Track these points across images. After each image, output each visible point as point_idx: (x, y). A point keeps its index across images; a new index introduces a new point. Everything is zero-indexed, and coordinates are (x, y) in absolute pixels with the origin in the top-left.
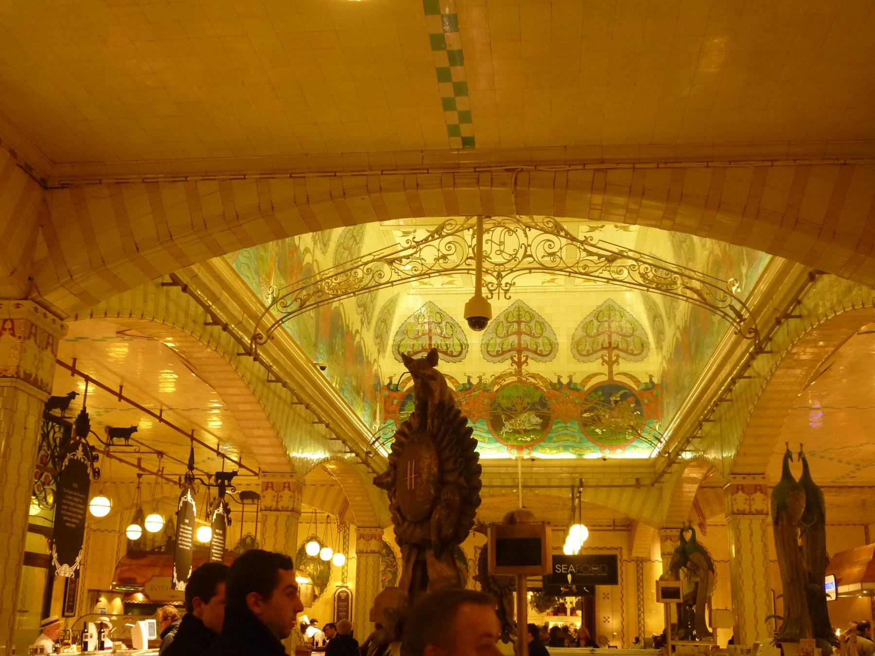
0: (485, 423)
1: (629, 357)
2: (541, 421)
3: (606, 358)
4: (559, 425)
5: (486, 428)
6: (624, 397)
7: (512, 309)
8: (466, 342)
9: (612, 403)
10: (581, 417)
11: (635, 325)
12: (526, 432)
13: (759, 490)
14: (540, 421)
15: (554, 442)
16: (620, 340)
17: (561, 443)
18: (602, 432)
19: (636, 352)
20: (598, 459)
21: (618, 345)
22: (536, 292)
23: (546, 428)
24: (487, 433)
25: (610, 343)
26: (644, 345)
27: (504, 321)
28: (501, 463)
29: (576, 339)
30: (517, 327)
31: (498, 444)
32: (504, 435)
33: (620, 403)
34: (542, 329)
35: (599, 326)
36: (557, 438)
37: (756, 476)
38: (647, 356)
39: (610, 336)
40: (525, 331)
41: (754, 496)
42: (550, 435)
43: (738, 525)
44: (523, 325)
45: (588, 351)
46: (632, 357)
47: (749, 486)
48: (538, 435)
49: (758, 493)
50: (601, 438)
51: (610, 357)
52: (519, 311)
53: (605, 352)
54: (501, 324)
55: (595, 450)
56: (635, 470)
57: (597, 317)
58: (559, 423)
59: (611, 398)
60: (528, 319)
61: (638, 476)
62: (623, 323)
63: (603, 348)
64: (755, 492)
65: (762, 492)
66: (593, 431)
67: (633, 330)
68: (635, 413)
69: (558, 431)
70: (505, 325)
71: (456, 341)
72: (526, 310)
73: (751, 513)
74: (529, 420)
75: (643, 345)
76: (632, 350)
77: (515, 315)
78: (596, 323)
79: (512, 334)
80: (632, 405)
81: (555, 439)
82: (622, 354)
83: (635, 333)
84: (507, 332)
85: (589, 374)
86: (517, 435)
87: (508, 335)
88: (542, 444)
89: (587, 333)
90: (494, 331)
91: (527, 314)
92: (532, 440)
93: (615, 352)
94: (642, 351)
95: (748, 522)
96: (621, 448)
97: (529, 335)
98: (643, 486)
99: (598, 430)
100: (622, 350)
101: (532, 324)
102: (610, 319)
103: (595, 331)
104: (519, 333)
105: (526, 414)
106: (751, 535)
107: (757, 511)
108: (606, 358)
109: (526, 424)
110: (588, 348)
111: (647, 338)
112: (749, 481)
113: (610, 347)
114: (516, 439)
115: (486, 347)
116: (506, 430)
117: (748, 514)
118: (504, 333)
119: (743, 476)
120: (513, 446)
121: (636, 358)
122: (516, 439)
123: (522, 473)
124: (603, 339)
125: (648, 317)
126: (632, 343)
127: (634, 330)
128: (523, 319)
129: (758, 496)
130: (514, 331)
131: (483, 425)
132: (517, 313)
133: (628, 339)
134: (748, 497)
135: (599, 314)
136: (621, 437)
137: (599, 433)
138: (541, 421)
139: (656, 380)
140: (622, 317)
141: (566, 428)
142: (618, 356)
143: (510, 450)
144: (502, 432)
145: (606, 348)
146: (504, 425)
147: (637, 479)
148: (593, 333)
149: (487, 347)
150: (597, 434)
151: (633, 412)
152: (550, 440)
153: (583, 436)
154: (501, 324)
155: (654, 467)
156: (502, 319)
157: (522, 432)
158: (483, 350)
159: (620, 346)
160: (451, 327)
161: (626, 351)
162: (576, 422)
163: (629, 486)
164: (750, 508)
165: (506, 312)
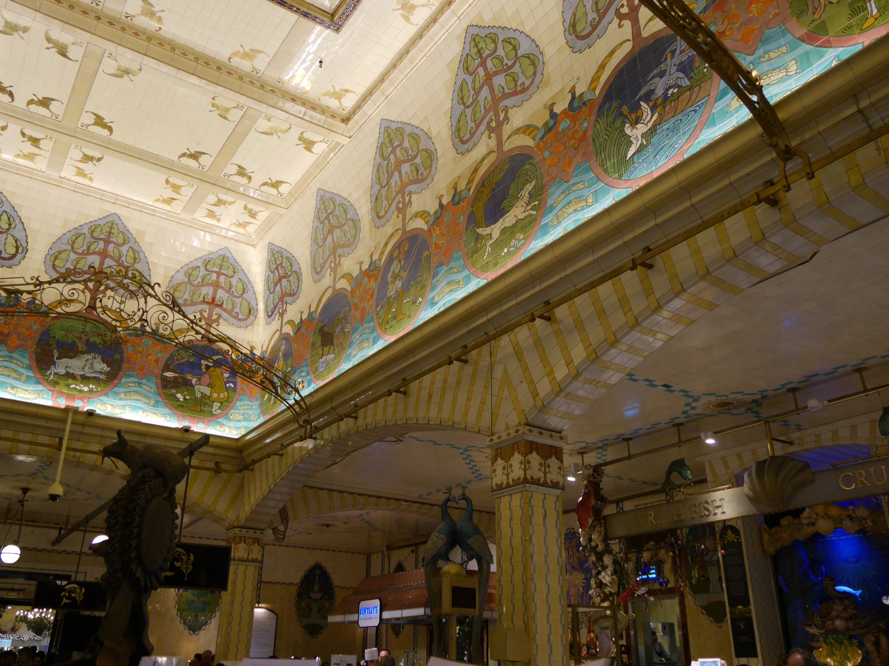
0: (27, 355)
1: (232, 320)
2: (108, 369)
3: (206, 315)
4: (131, 379)
5: (27, 362)
6: (218, 364)
7: (102, 223)
8: (24, 245)
9: (203, 367)
10: (162, 375)
11: (246, 286)
12: (85, 379)
14: (105, 367)
15: (120, 399)
16: (226, 298)
17: (129, 402)
18: (185, 399)
19: (241, 316)
20: (176, 429)
21: (223, 303)
22: (141, 211)
23: (114, 379)
24: (26, 368)
25: (214, 299)
26: (251, 311)
27: (87, 233)
28: (41, 411)
29: (175, 282)
30: (102, 247)
31: (40, 387)
32: (52, 377)
33: (212, 369)
34: (135, 259)
35: (206, 276)
36: (125, 395)
38: (252, 324)
39: (215, 292)
40: (112, 254)
41: (549, 461)
42: (116, 389)
43: (530, 499)
44: (111, 247)
45: (186, 300)
46: (235, 321)
47: (543, 445)
48: (99, 386)
49: (554, 459)
50: (182, 406)
51: (210, 315)
52: (111, 228)
53: (206, 307)
54: (83, 236)
55: (172, 419)
56: (218, 451)
57: (206, 265)
59: (202, 361)
60: (121, 241)
61: (218, 459)
62: (234, 281)
63: (204, 302)
65: (557, 458)
66: (174, 396)
67: (244, 290)
68: (228, 385)
69: (129, 386)
70: (87, 240)
71: (10, 240)
72: (121, 230)
73: (545, 484)
74: (92, 364)
75: (250, 311)
76: (236, 313)
77: (104, 231)
78: (203, 272)
79: (94, 253)
80: (226, 375)
81: (122, 395)
82: (224, 314)
83: (245, 295)
84: (88, 248)
85: (180, 328)
86: (70, 381)
87: (88, 252)
88: (103, 398)
89: (189, 280)
90: (70, 243)
91: (121, 235)
92: (91, 391)
93: (217, 310)
94: (248, 317)
95: (541, 497)
96: (204, 423)
97: (116, 261)
98: (226, 471)
99: (179, 396)
100: (225, 310)
101: (124, 249)
102: (221, 269)
103: (200, 280)
104: (104, 254)
105: (89, 357)
106: (545, 517)
107: (552, 482)
108: (206, 315)
109: (87, 369)
110: (186, 296)
111: (257, 305)
112: (546, 440)
113: (213, 303)
114: (68, 385)
115: (52, 260)
116: (56, 371)
118: (82, 249)
119: (539, 430)
120: (61, 394)
121: (243, 324)
122: (68, 385)
123: (71, 431)
124: (208, 291)
125: (267, 279)
126: (239, 306)
127: (243, 293)
128: (114, 240)
129: (553, 461)
130: (97, 250)
131: (24, 357)
132: (108, 230)
133: (235, 299)
134: (543, 461)
135: (209, 261)
136: (207, 408)
137: (181, 399)
138: (108, 369)
139: (258, 352)
140: (234, 272)
141: (139, 384)
142: (220, 316)
143: (57, 398)
144: (49, 372)
145: (208, 303)
146: (54, 364)
147: (217, 463)
148: (196, 283)
149: (56, 259)
150: (178, 400)
151: (226, 383)
152: (116, 394)
153: (160, 399)
154: (83, 236)
155: (241, 452)
156: (85, 230)
157: (79, 378)
158: (48, 261)
159: (224, 305)
160: (9, 219)
161: (229, 313)
163: (205, 469)
165: (94, 223)
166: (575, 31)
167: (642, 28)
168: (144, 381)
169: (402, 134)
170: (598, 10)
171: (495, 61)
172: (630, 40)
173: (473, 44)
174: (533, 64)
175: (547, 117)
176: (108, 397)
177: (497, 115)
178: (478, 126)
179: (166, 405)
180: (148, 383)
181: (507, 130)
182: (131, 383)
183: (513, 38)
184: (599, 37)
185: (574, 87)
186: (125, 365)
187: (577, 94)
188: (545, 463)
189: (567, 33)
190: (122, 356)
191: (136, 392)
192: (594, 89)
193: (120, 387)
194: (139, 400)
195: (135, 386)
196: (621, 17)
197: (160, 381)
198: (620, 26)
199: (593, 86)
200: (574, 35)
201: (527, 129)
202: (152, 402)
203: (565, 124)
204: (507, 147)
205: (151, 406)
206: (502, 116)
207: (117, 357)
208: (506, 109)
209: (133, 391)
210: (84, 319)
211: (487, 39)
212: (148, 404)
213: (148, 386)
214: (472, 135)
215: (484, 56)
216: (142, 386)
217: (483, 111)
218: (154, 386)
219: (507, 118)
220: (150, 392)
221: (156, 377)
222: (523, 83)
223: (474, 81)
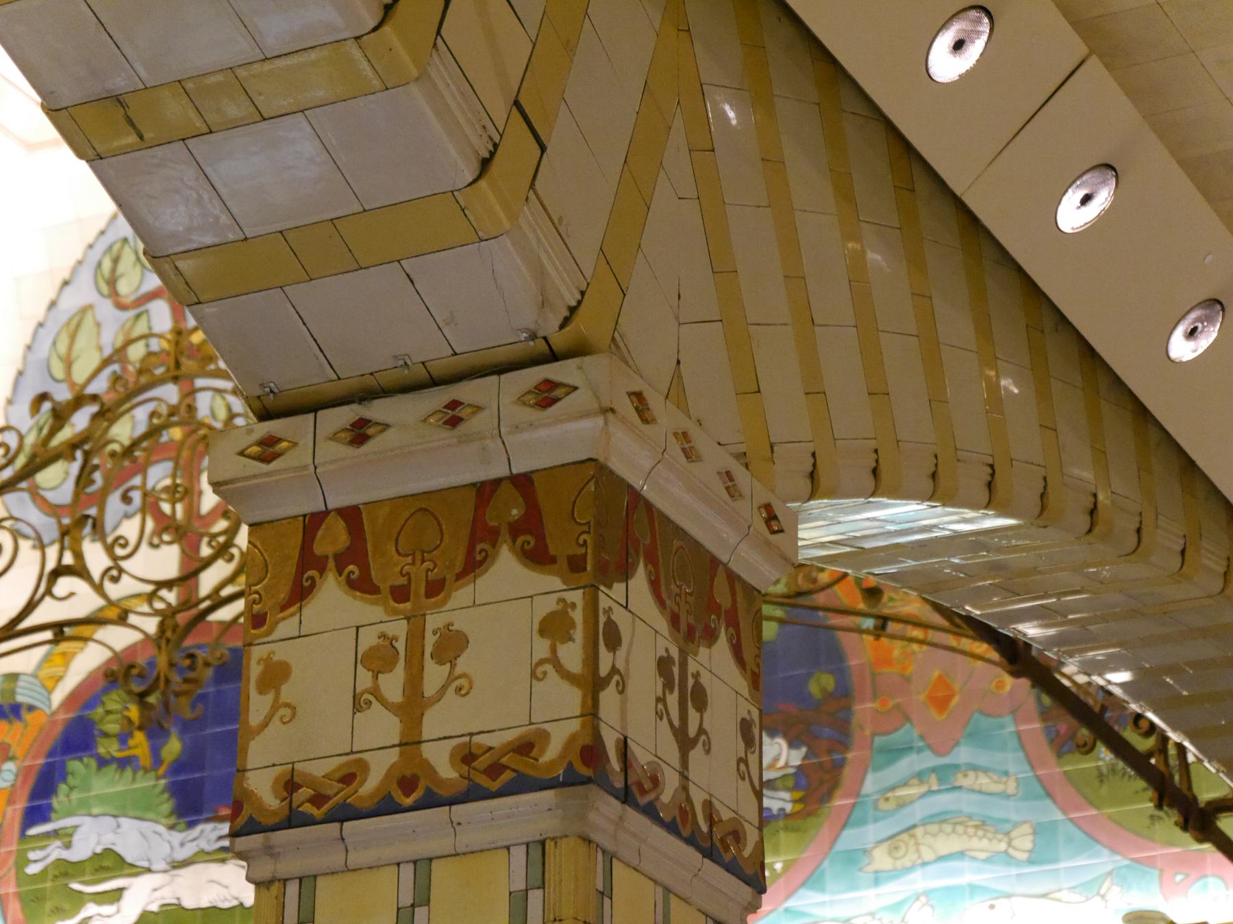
13: (516, 530)
15: (878, 879)
17: (919, 881)
23: (828, 796)
37: (466, 391)
42: (849, 838)
58: (907, 749)
64: (473, 566)
69: (902, 804)
81: (881, 860)
117: (386, 807)
119: (344, 416)
141: (946, 775)
152: (855, 858)
153: (1059, 816)
162: (1010, 727)
164: (410, 743)
168: (963, 754)
176: (822, 890)
179: (1093, 834)
180: (982, 759)
182: (905, 784)
186: (863, 710)
188: (416, 636)
190: (841, 673)
191: (940, 819)
193: (862, 822)
194: (961, 854)
195: (930, 792)
197: (1037, 725)
202: (1023, 840)
205: (1018, 863)
207: (822, 683)
209: (926, 822)
210: (48, 635)
212: (1007, 858)
213: (986, 771)
216: (961, 781)
218: (1014, 762)
220: (1006, 796)
221: (1013, 712)
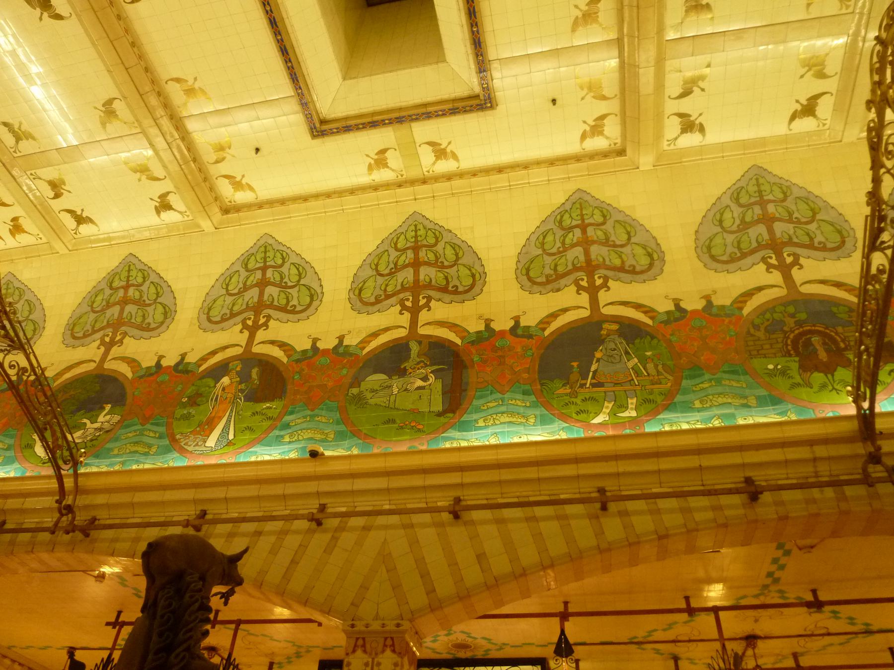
166: (208, 313)
167: (255, 343)
169: (20, 296)
170: (231, 310)
171: (137, 293)
172: (242, 347)
173: (127, 268)
174: (165, 314)
175: (153, 364)
177: (115, 334)
178: (94, 332)
181: (115, 351)
183: (161, 286)
184: (222, 329)
185: (185, 354)
187: (186, 361)
189: (202, 310)
192: (200, 366)
196: (245, 326)
198: (241, 332)
199: (200, 363)
200: (206, 316)
201: (132, 362)
203: (165, 377)
204: (109, 365)
206: (118, 338)
208: (125, 334)
211: (140, 273)
214: (85, 336)
215: (130, 282)
217: (105, 323)
219: (121, 342)
222: (149, 324)
223: (111, 295)
